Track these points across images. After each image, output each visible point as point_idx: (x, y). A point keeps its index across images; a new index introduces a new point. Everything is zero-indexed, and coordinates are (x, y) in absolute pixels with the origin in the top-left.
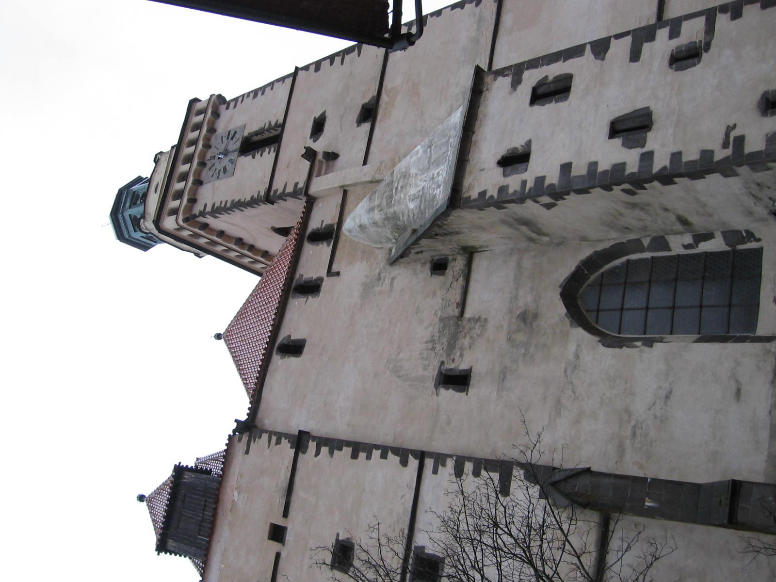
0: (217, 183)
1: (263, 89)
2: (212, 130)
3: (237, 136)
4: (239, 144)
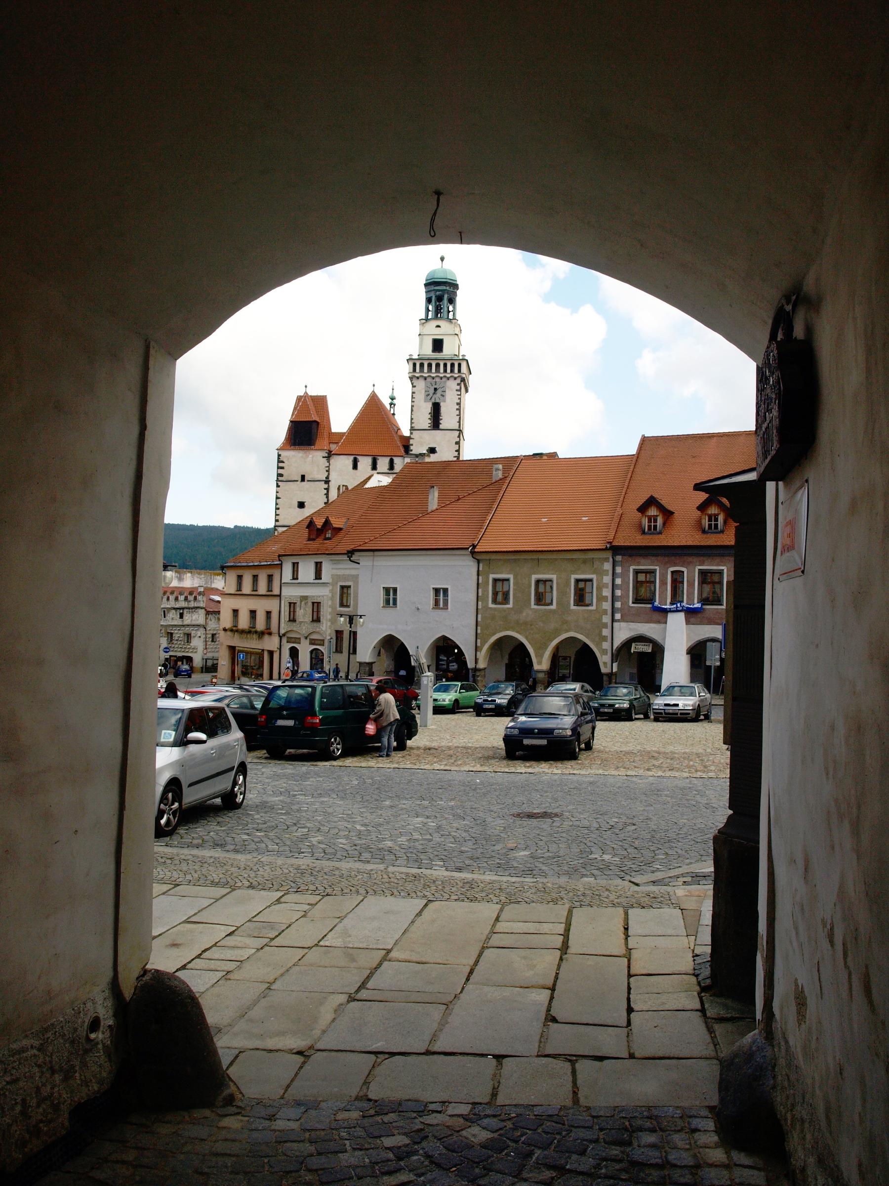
0: (423, 391)
1: (459, 409)
2: (448, 379)
3: (442, 398)
4: (437, 401)
